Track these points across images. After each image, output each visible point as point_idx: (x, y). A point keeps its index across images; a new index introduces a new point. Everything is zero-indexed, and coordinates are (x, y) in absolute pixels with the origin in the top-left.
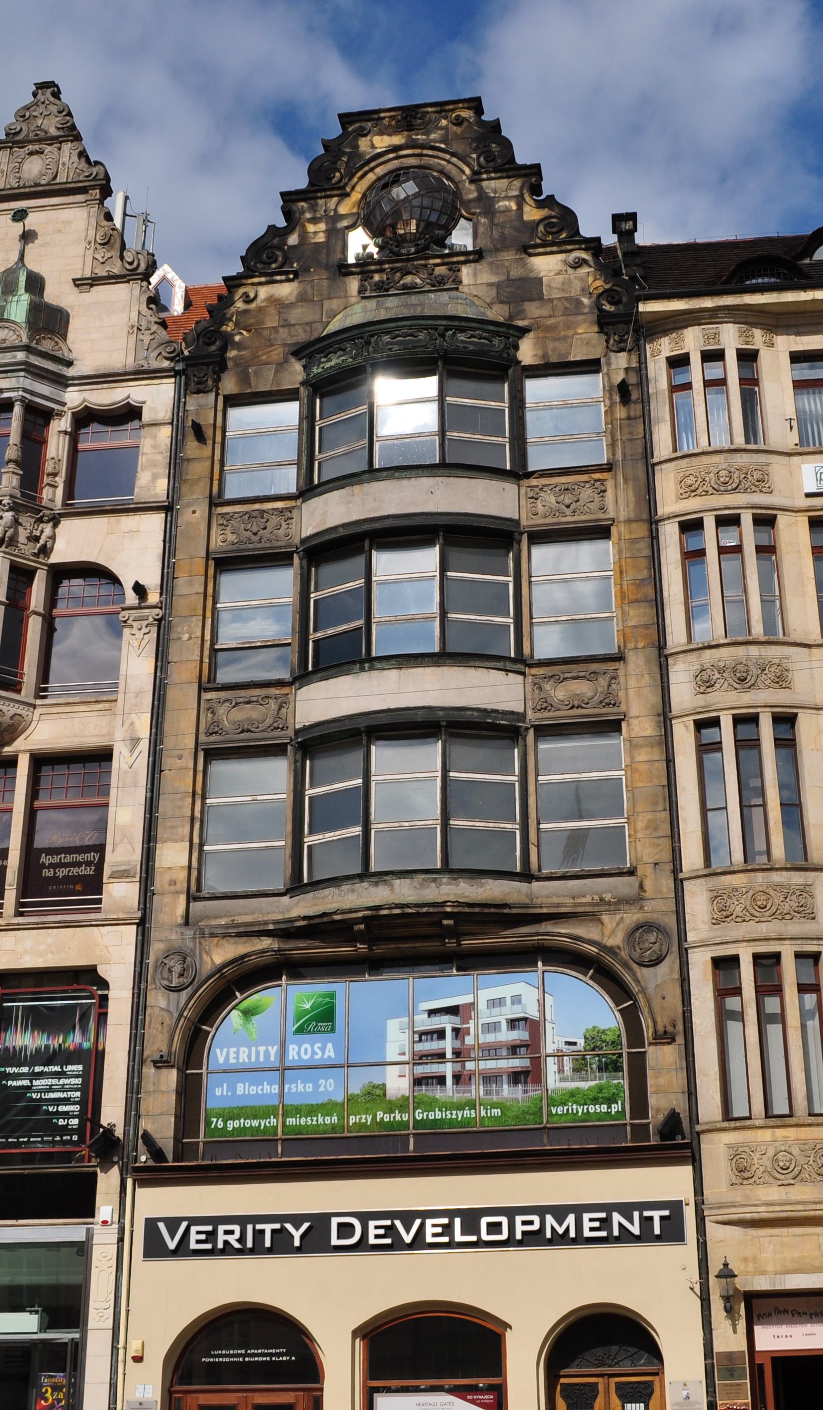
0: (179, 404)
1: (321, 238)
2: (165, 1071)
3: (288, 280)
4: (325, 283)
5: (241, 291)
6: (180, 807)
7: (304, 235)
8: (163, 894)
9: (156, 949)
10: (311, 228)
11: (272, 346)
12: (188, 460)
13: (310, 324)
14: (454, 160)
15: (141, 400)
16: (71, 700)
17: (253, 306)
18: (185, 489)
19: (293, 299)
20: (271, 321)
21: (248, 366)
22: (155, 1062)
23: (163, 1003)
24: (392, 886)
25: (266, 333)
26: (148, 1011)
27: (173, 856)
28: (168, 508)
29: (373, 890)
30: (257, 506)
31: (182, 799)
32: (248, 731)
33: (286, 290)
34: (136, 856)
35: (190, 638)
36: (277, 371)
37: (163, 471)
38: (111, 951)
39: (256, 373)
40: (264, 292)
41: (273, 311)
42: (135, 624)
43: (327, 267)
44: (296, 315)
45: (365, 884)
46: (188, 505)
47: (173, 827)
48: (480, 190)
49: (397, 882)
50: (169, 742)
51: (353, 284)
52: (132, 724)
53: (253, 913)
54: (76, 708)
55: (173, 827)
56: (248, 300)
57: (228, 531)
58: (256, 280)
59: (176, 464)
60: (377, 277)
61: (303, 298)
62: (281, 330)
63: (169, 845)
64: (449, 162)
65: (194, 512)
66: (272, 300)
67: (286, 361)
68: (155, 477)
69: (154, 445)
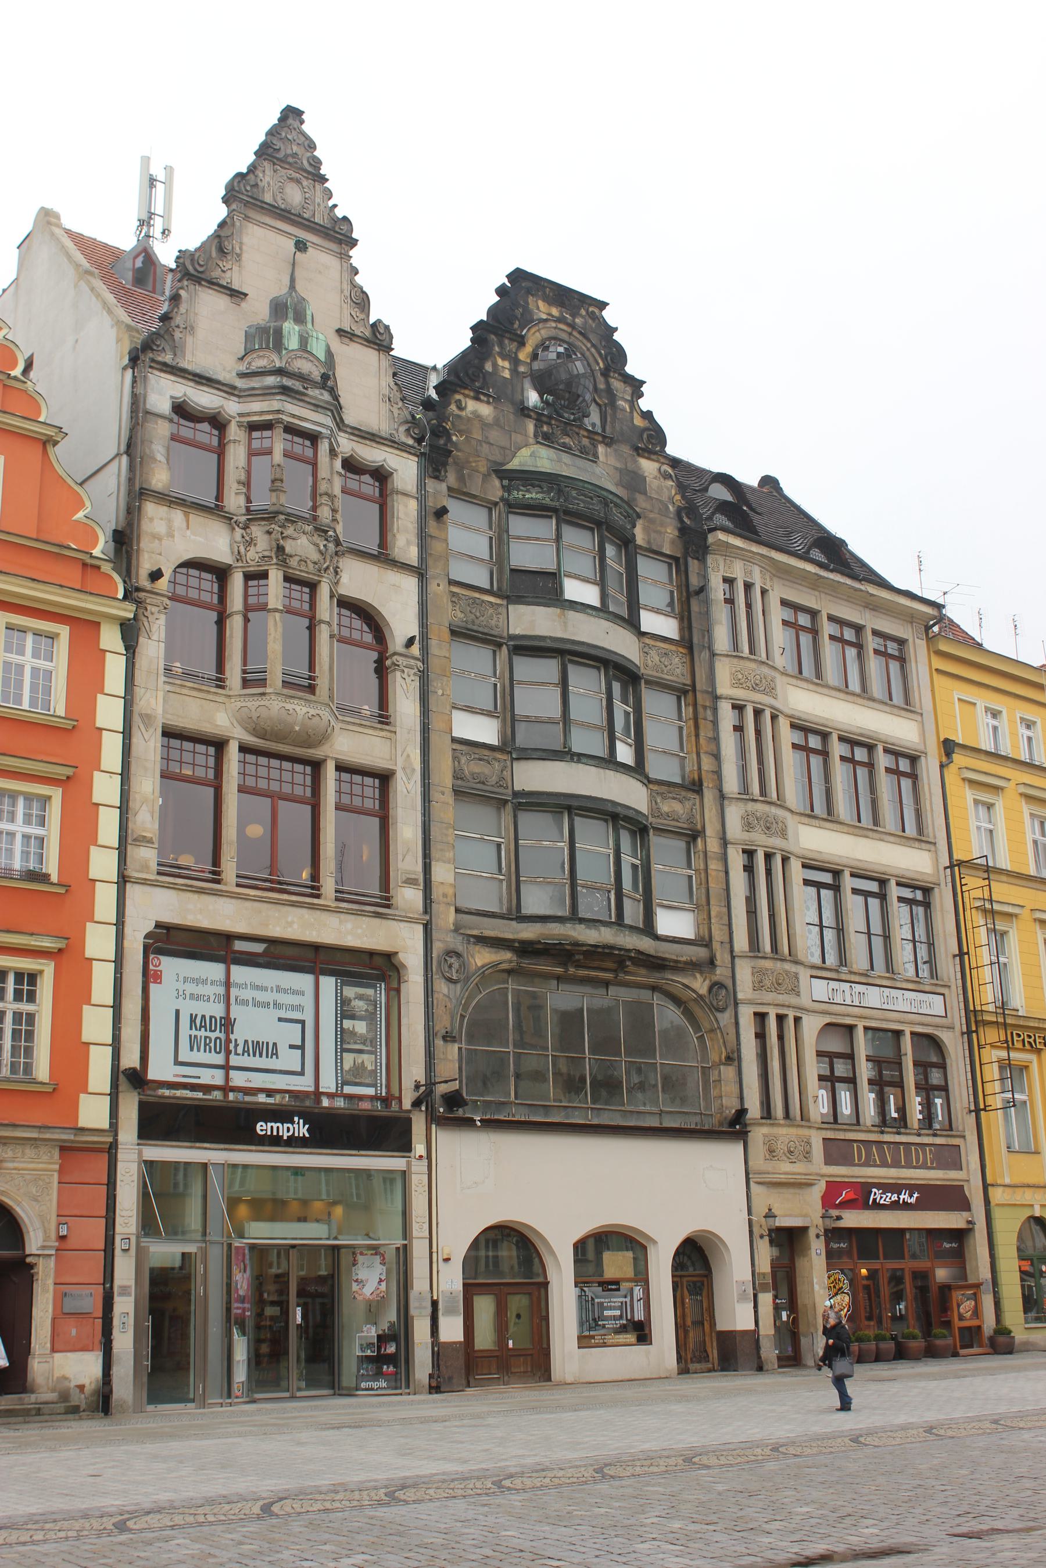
0: (421, 485)
1: (507, 374)
2: (450, 1045)
3: (488, 403)
4: (512, 417)
5: (458, 397)
6: (446, 835)
7: (495, 365)
8: (439, 903)
9: (438, 947)
10: (500, 362)
11: (479, 456)
12: (431, 536)
13: (503, 448)
14: (593, 350)
15: (393, 466)
16: (363, 722)
17: (463, 414)
18: (430, 562)
19: (490, 420)
20: (477, 435)
21: (463, 468)
22: (444, 1038)
23: (445, 991)
24: (599, 930)
25: (474, 442)
26: (435, 996)
27: (442, 873)
28: (420, 573)
29: (588, 931)
30: (477, 595)
31: (447, 828)
32: (483, 783)
33: (485, 410)
34: (419, 868)
35: (443, 695)
36: (483, 481)
37: (414, 539)
38: (408, 944)
39: (469, 476)
40: (471, 405)
41: (477, 424)
42: (406, 670)
43: (513, 403)
44: (494, 435)
45: (583, 926)
46: (435, 578)
47: (442, 850)
48: (608, 384)
49: (603, 929)
50: (434, 779)
51: (530, 426)
52: (408, 756)
53: (494, 929)
54: (366, 731)
55: (442, 850)
56: (460, 408)
57: (457, 608)
58: (467, 392)
59: (423, 539)
60: (545, 428)
61: (497, 423)
62: (484, 444)
63: (440, 864)
64: (588, 349)
65: (438, 585)
66: (477, 416)
67: (489, 475)
68: (408, 543)
69: (406, 513)
